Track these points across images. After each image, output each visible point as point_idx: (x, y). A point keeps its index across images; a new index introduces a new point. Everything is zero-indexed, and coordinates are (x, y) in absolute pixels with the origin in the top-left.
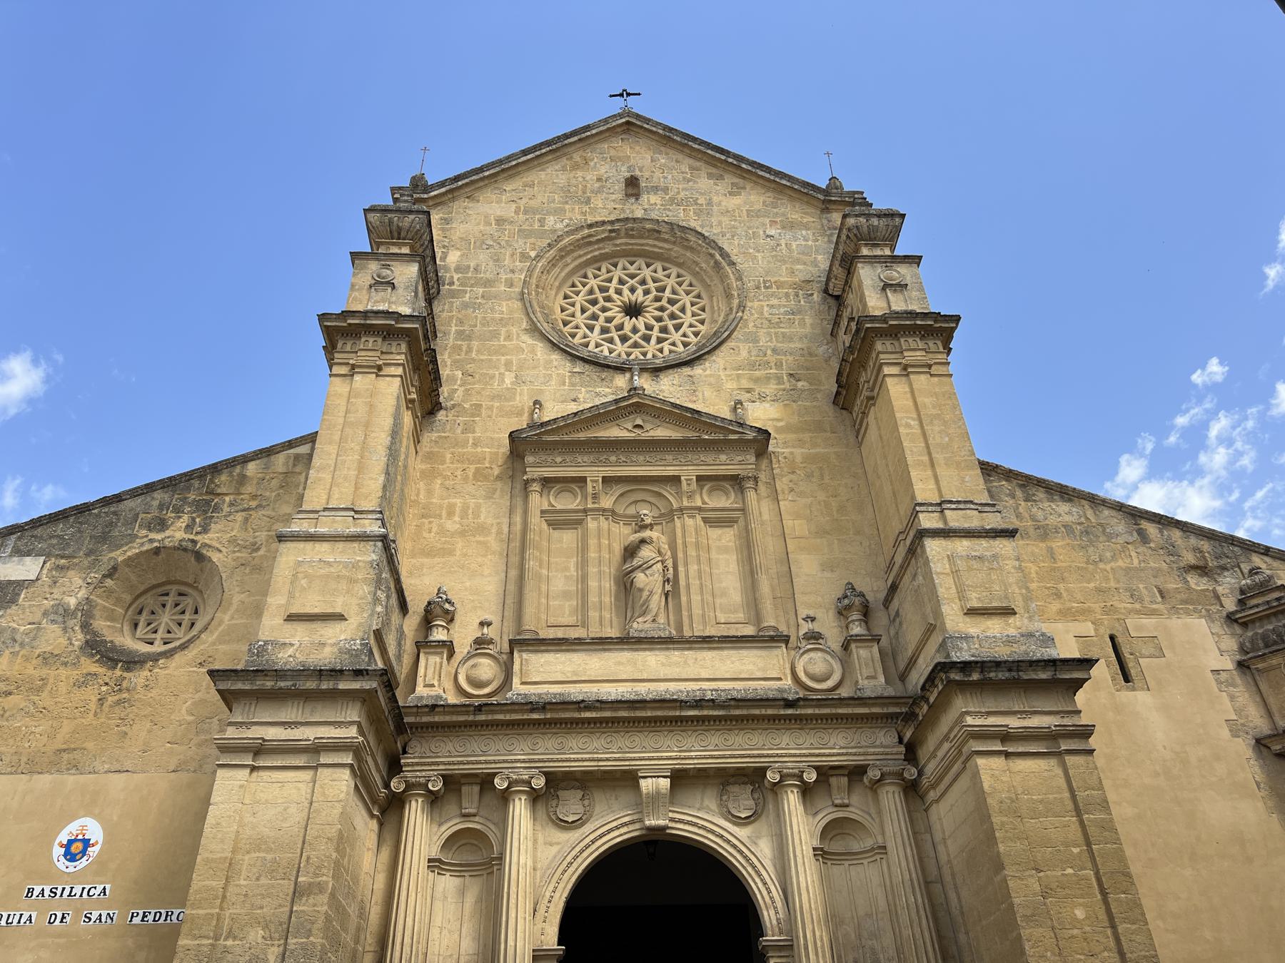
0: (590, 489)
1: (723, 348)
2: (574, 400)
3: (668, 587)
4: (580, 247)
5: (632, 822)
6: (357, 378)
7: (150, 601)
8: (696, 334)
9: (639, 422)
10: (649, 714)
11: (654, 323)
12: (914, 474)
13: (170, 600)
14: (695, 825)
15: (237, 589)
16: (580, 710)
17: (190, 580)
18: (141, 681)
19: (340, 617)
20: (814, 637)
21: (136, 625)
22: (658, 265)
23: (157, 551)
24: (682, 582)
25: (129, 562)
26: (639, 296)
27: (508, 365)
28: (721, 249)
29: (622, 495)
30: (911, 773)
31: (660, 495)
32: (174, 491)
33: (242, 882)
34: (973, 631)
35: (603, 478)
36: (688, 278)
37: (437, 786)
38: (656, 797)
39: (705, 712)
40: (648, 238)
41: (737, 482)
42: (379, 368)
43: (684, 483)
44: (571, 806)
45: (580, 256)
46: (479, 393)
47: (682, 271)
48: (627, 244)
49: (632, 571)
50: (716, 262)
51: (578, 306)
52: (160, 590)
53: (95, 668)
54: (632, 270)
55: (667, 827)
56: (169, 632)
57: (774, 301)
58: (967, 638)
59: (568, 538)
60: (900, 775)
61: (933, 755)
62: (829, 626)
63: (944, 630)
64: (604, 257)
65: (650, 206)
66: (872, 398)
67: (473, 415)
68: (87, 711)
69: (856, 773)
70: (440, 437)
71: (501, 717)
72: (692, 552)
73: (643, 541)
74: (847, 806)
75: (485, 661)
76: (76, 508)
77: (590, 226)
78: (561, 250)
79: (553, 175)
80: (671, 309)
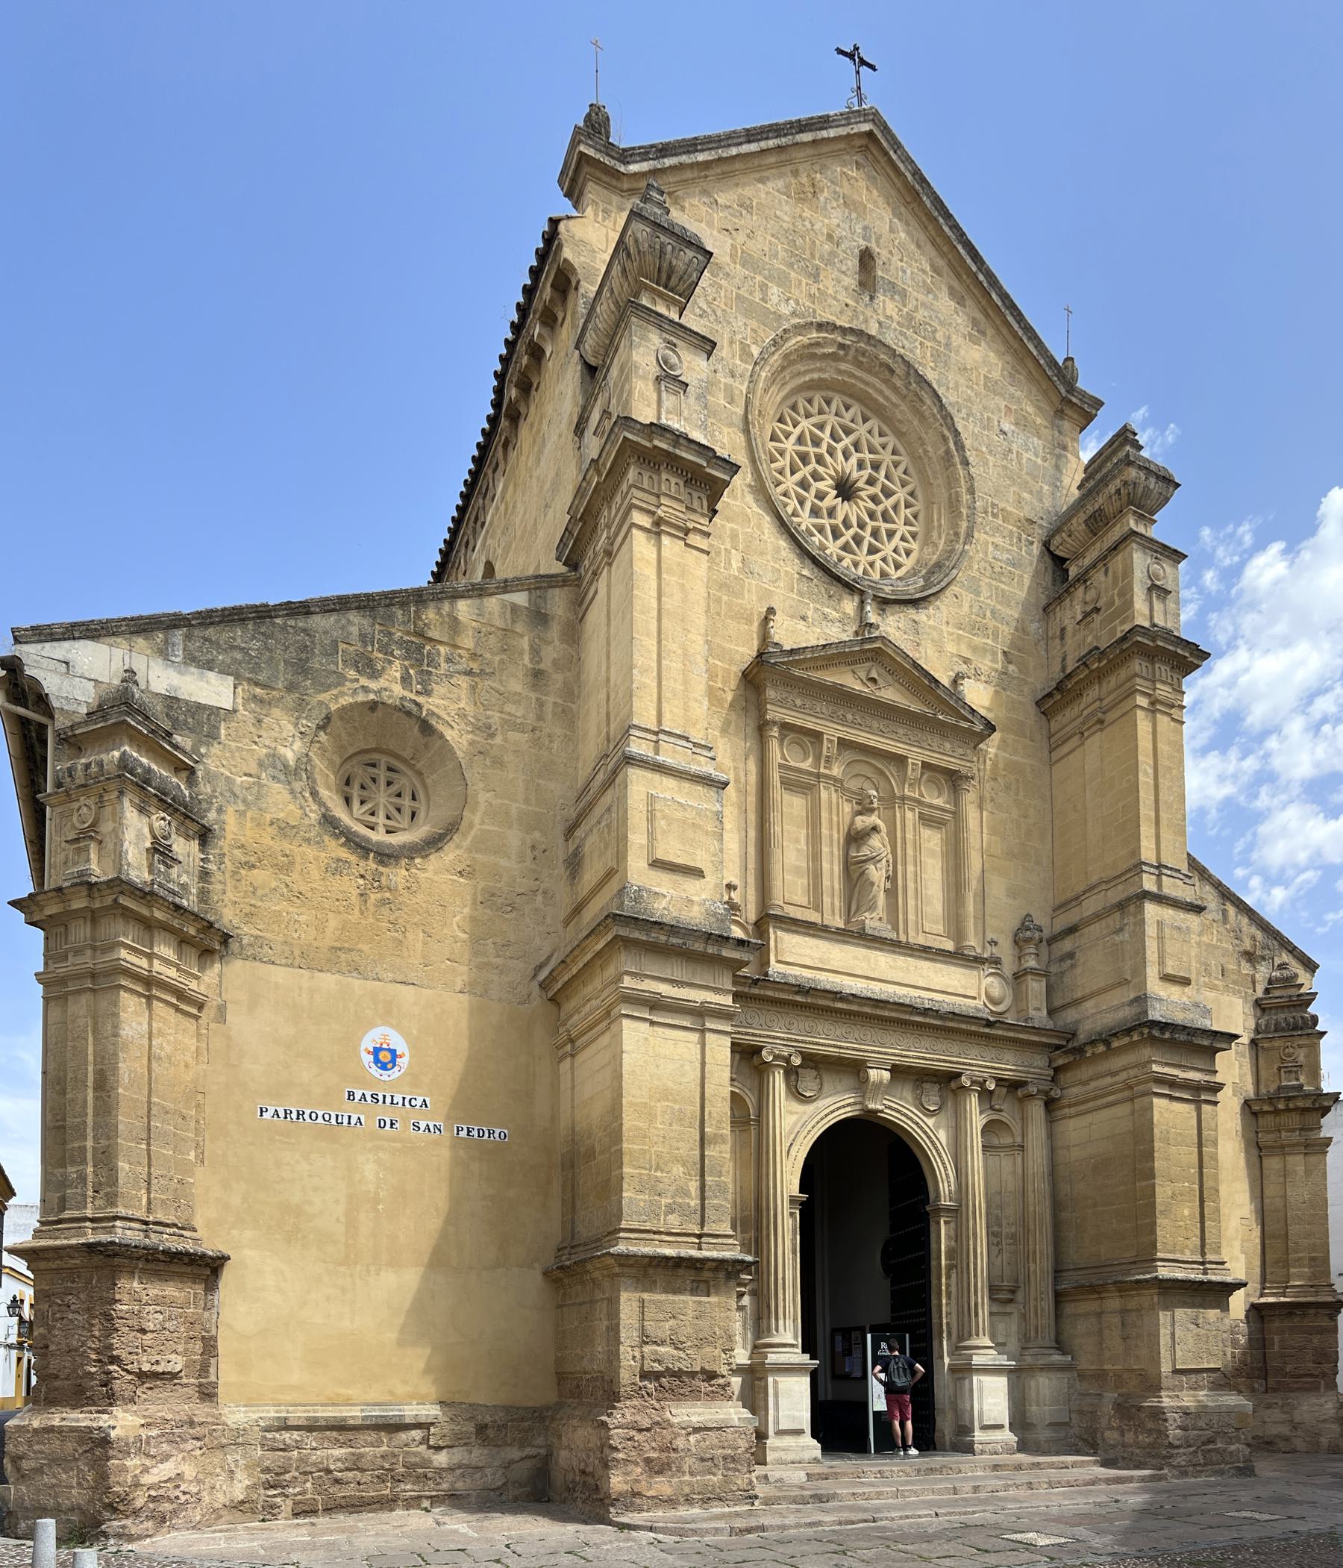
5: (854, 1104)
15: (481, 785)
16: (834, 1000)
27: (734, 536)
39: (927, 1020)
40: (876, 375)
54: (876, 441)
71: (770, 993)
76: (254, 608)
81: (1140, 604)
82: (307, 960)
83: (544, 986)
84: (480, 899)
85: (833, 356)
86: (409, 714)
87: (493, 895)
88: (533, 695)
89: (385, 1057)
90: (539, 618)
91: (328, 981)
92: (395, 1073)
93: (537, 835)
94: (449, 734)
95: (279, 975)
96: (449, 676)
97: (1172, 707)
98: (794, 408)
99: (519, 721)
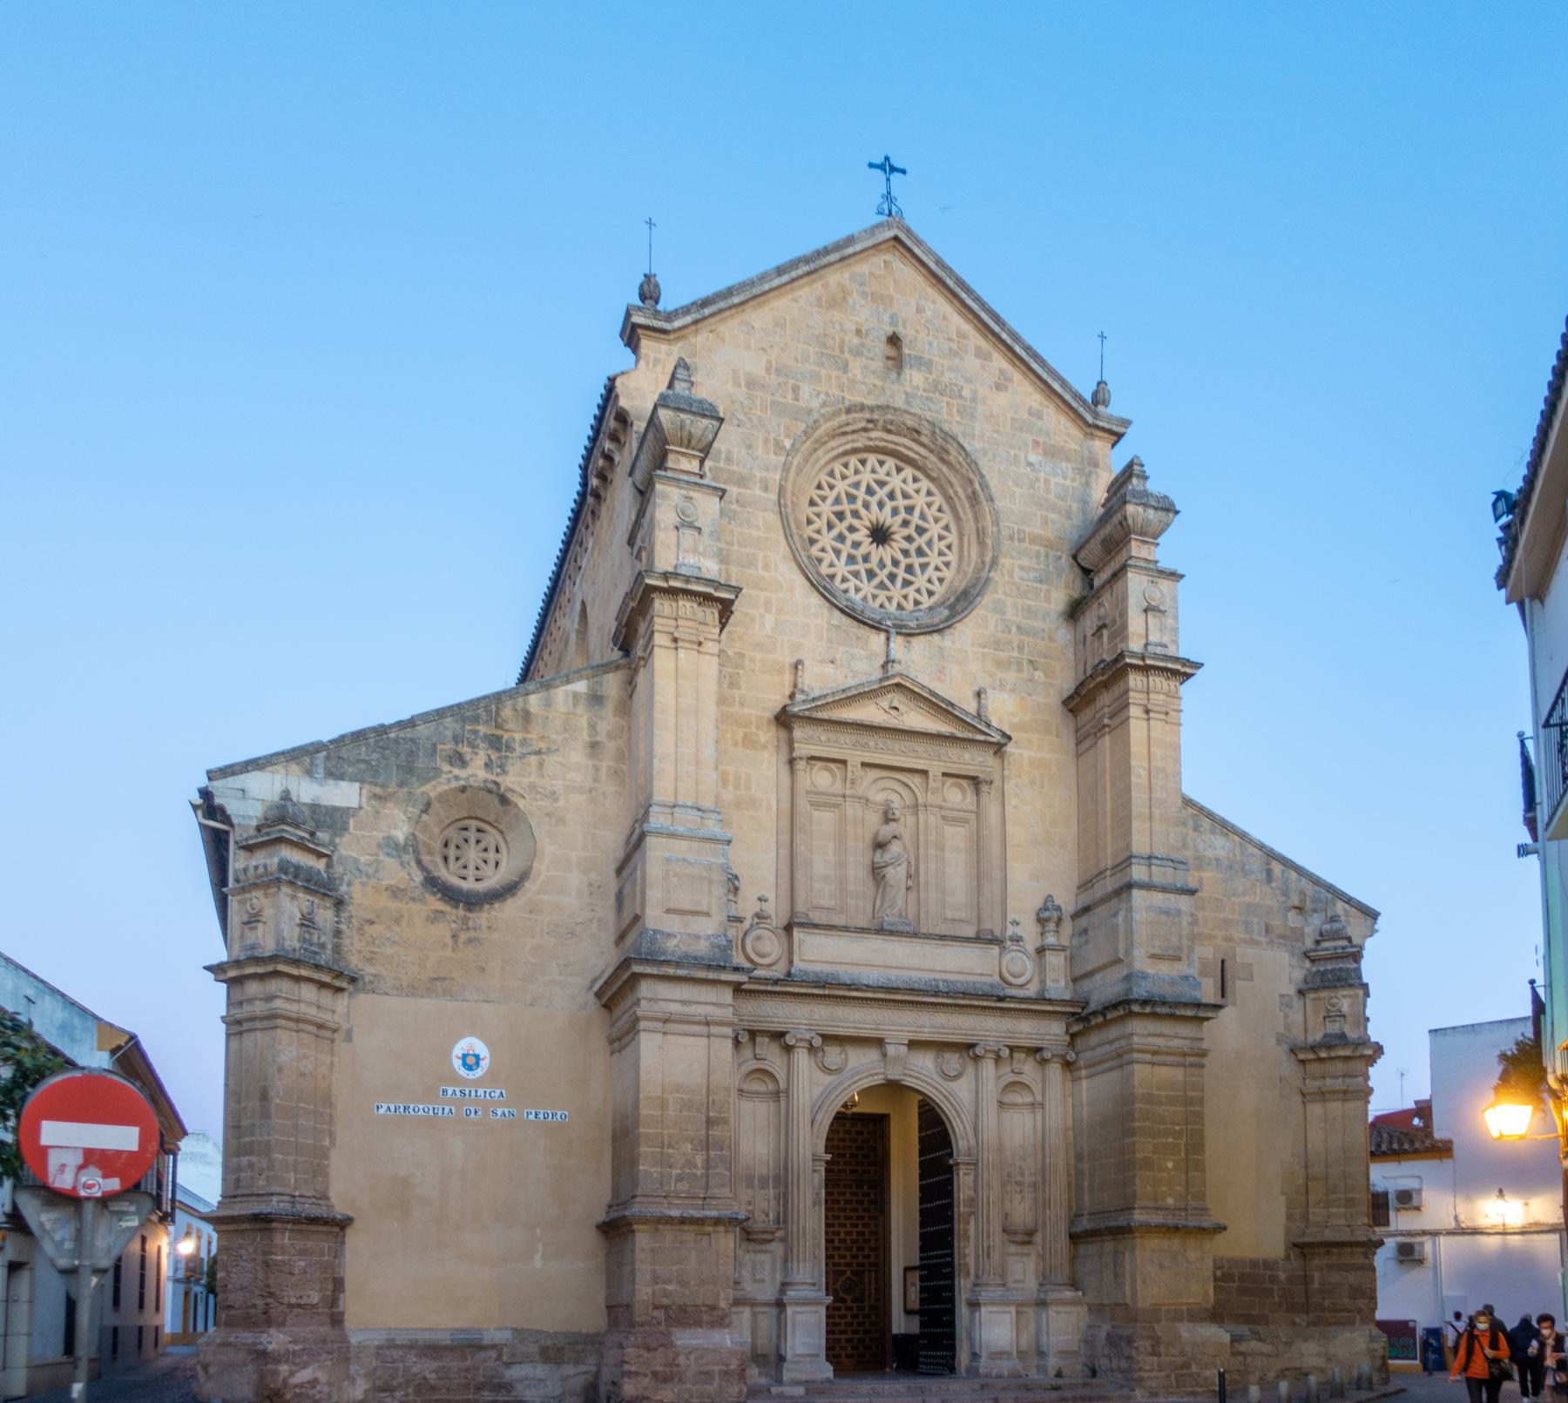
0: (849, 775)
9: (895, 704)
17: (491, 819)
18: (484, 923)
21: (446, 859)
22: (909, 472)
24: (922, 880)
26: (893, 523)
28: (982, 476)
31: (906, 785)
34: (1151, 971)
36: (938, 499)
38: (896, 1058)
41: (975, 781)
46: (741, 638)
47: (934, 489)
50: (974, 492)
52: (461, 824)
53: (441, 906)
57: (1026, 562)
58: (1145, 977)
59: (825, 818)
63: (1130, 964)
67: (736, 667)
68: (445, 945)
72: (932, 852)
79: (798, 305)
81: (1135, 622)
82: (413, 990)
83: (598, 995)
85: (865, 430)
86: (490, 792)
88: (590, 763)
89: (471, 1060)
90: (596, 699)
91: (428, 1004)
92: (479, 1073)
93: (593, 875)
94: (521, 803)
95: (392, 1002)
96: (523, 756)
97: (1170, 714)
98: (831, 474)
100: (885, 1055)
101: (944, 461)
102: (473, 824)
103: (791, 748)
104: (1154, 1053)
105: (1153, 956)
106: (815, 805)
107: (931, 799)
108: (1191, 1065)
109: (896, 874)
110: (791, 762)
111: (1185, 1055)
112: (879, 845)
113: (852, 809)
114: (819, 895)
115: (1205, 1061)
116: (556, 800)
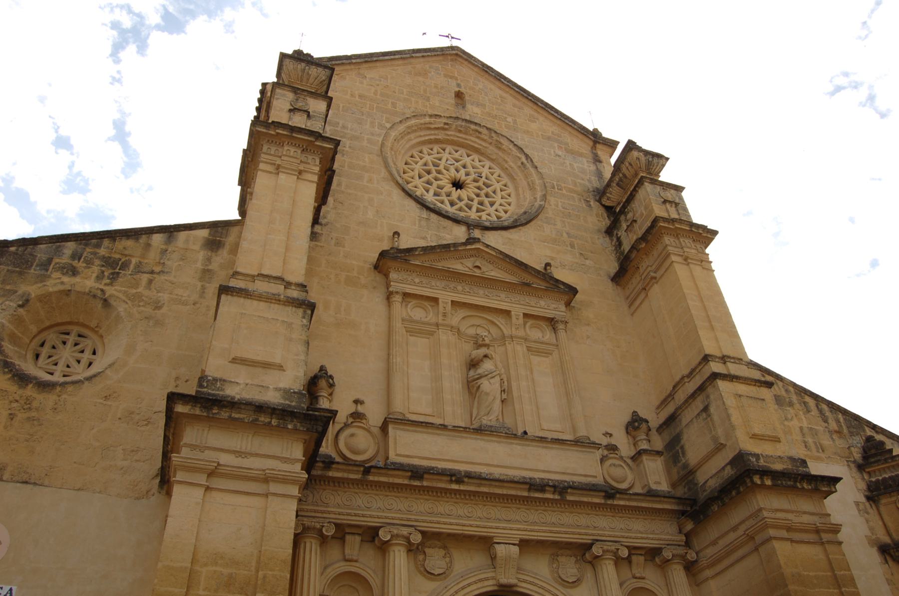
1: (533, 222)
2: (423, 238)
3: (504, 396)
4: (421, 129)
6: (282, 176)
7: (52, 337)
8: (506, 212)
9: (478, 264)
10: (505, 492)
11: (475, 197)
12: (701, 333)
13: (71, 339)
14: (535, 585)
17: (93, 324)
19: (280, 368)
20: (612, 448)
21: (37, 356)
22: (476, 157)
23: (68, 293)
25: (44, 299)
29: (463, 318)
30: (691, 556)
32: (86, 245)
33: (201, 592)
34: (757, 450)
35: (452, 301)
36: (498, 171)
37: (329, 531)
40: (471, 135)
41: (552, 322)
42: (300, 172)
43: (514, 318)
44: (435, 559)
45: (421, 136)
47: (493, 165)
48: (454, 136)
49: (478, 379)
50: (522, 163)
51: (417, 173)
55: (516, 586)
56: (68, 366)
59: (420, 344)
60: (683, 557)
61: (714, 543)
62: (621, 440)
64: (437, 141)
65: (473, 111)
66: (655, 278)
69: (653, 553)
70: (317, 246)
73: (486, 356)
74: (644, 578)
75: (360, 433)
77: (431, 116)
78: (409, 127)
80: (486, 190)
84: (119, 415)
87: (132, 413)
88: (199, 284)
99: (184, 299)
100: (493, 558)
101: (500, 148)
102: (75, 330)
103: (388, 286)
104: (789, 529)
105: (754, 436)
106: (411, 332)
107: (514, 332)
108: (828, 542)
109: (490, 387)
110: (389, 296)
111: (817, 531)
112: (473, 364)
113: (444, 336)
114: (415, 401)
115: (840, 536)
116: (158, 308)
